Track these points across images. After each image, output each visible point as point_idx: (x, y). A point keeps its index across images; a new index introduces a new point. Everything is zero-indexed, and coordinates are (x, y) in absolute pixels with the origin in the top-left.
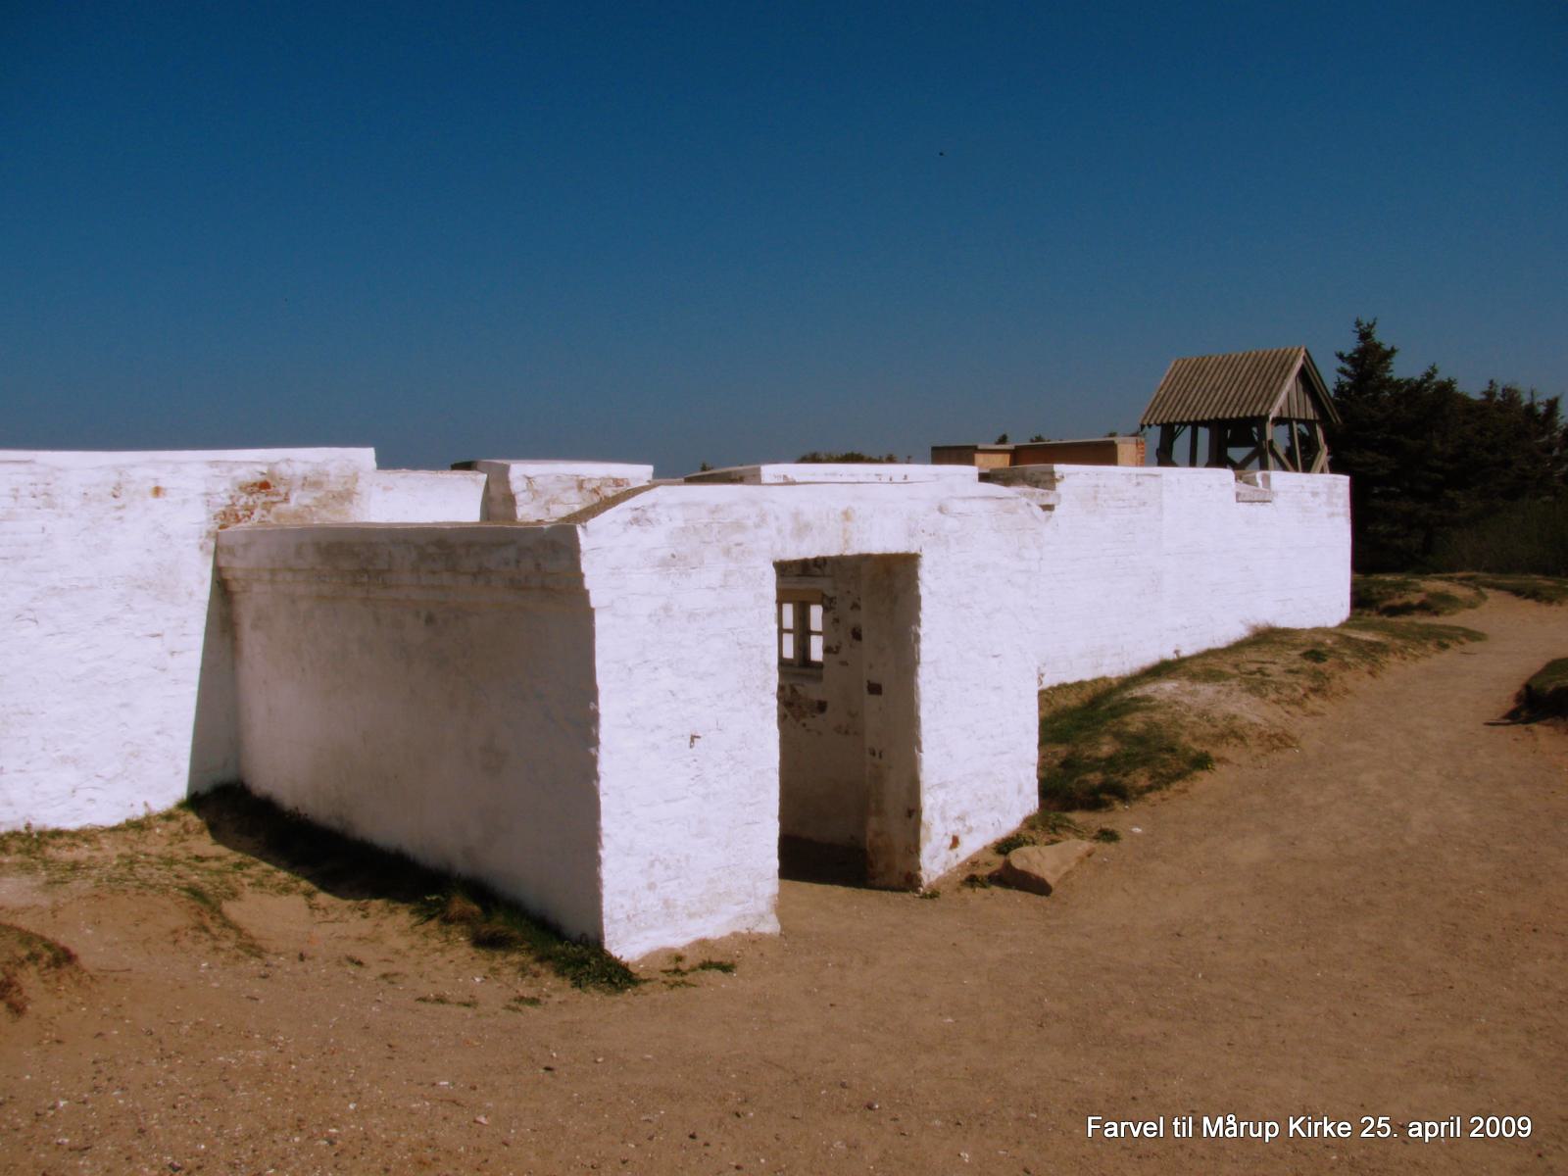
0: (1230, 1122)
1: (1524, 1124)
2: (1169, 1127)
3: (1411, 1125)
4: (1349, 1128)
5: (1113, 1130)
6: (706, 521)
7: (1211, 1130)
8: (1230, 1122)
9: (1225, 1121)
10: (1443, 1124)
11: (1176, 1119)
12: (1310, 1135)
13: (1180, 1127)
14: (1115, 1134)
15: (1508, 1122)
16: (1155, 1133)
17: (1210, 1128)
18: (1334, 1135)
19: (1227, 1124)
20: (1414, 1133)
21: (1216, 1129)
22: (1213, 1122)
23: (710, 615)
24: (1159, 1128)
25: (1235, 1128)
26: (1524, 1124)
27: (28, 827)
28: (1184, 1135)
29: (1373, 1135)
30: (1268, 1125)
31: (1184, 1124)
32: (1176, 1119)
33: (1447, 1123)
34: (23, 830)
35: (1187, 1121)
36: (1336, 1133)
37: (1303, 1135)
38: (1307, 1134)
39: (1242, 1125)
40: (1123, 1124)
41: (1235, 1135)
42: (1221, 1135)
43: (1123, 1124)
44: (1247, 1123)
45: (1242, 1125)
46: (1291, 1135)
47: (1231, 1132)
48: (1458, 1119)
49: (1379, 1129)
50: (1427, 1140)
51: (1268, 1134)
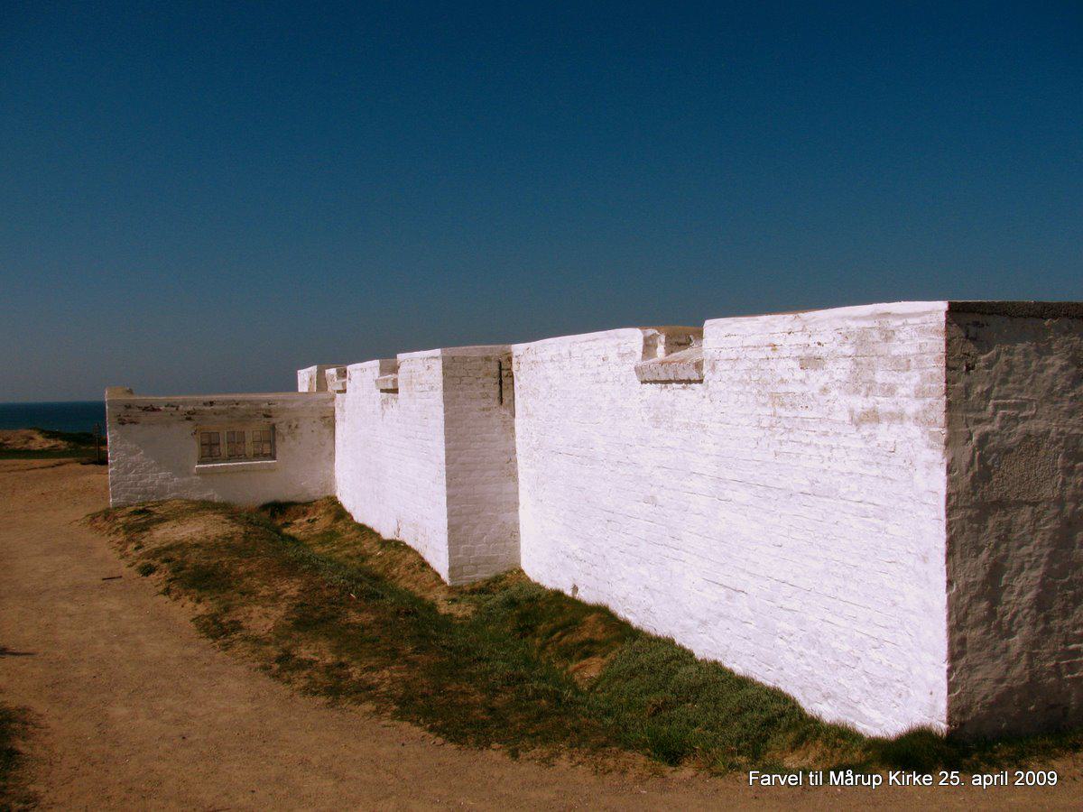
1: (1052, 776)
9: (845, 774)
13: (814, 778)
14: (769, 783)
16: (796, 783)
18: (920, 784)
22: (837, 776)
26: (1052, 776)
30: (874, 777)
35: (818, 774)
38: (901, 783)
39: (857, 776)
40: (774, 776)
43: (774, 776)
45: (857, 776)
51: (874, 783)
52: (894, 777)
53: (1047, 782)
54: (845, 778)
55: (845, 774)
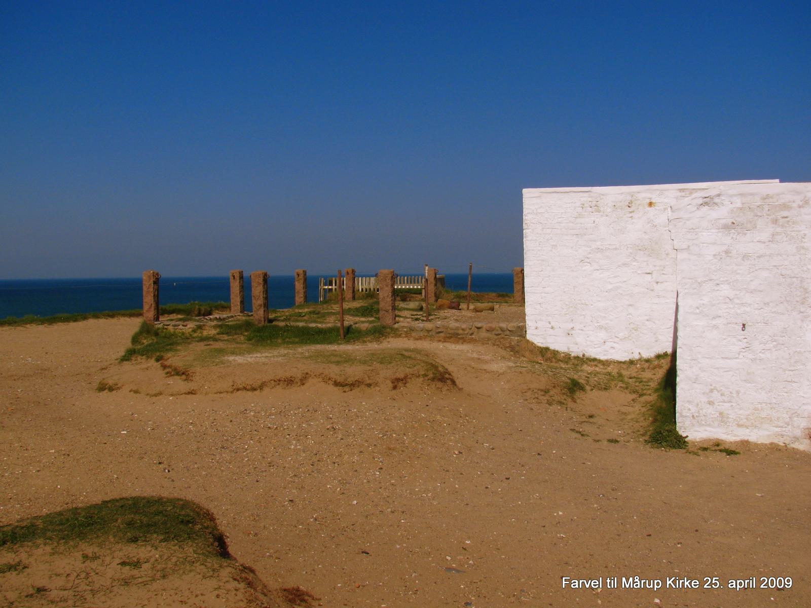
0: (636, 580)
1: (788, 581)
2: (605, 583)
3: (730, 582)
4: (698, 583)
5: (576, 584)
6: (758, 204)
7: (626, 584)
8: (636, 580)
9: (634, 580)
10: (746, 581)
11: (608, 579)
12: (677, 587)
13: (610, 583)
16: (597, 586)
17: (626, 583)
18: (690, 587)
19: (635, 581)
21: (629, 584)
22: (627, 580)
23: (759, 257)
24: (599, 583)
25: (639, 583)
26: (788, 581)
27: (584, 355)
28: (612, 587)
29: (710, 587)
30: (656, 582)
31: (612, 581)
32: (608, 579)
33: (749, 581)
34: (581, 356)
35: (614, 580)
36: (691, 586)
37: (674, 587)
38: (676, 586)
39: (643, 581)
40: (581, 581)
41: (639, 587)
42: (632, 587)
43: (581, 581)
44: (645, 581)
45: (643, 581)
46: (668, 587)
49: (713, 584)
51: (656, 586)
53: (784, 586)
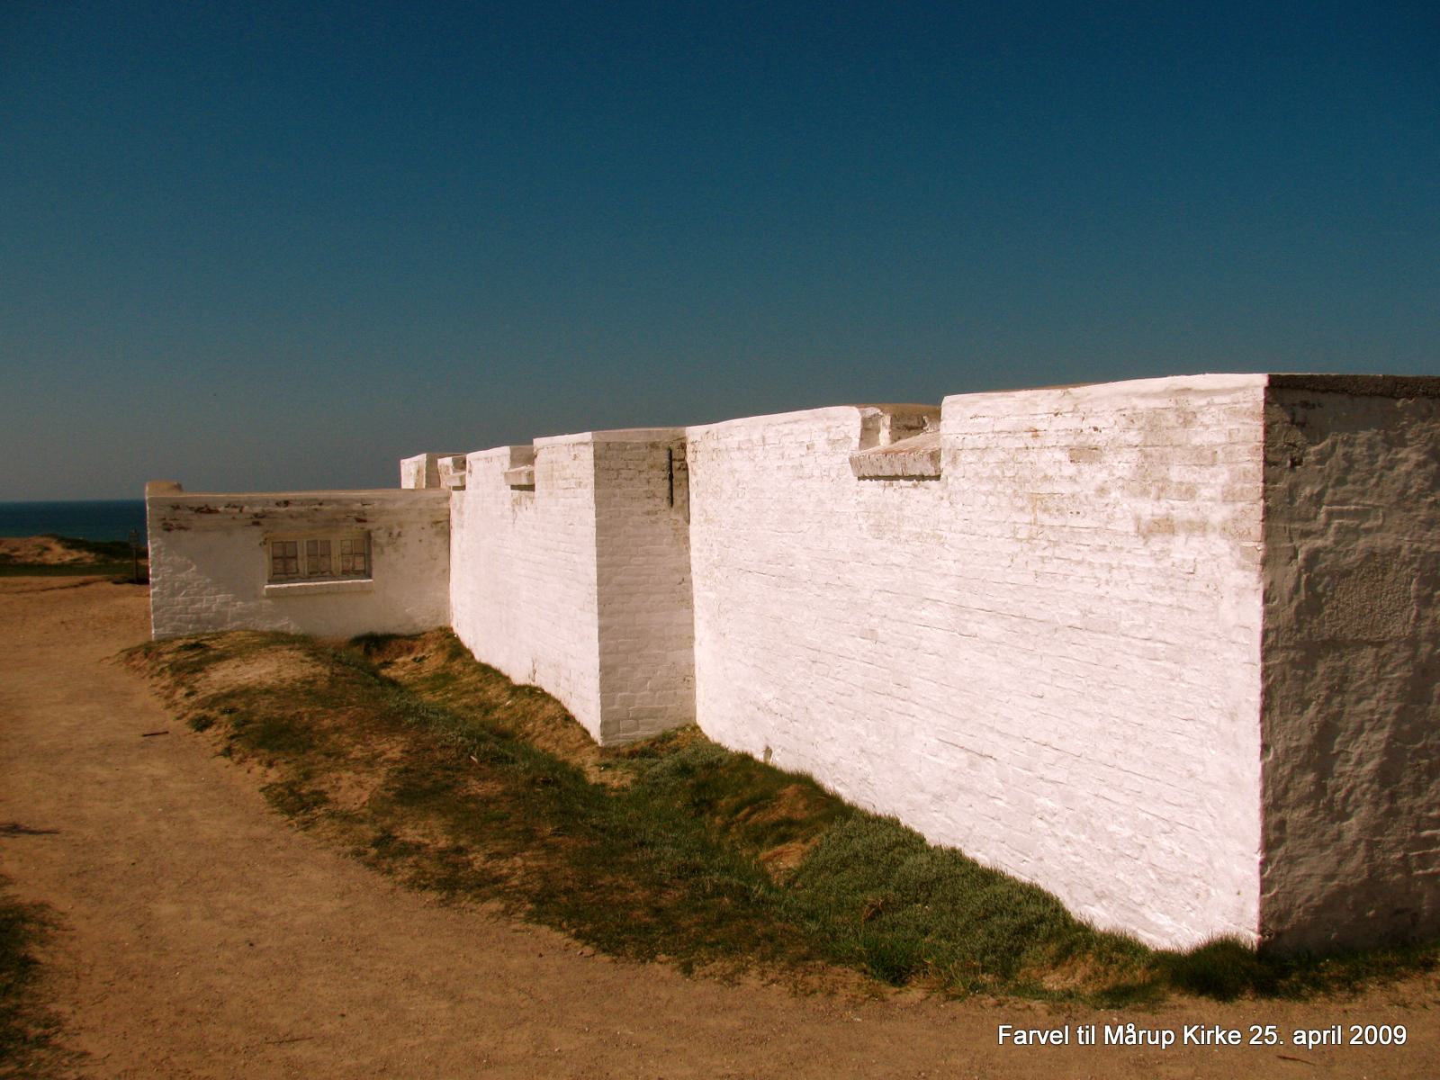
0: (1129, 1031)
1: (1400, 1032)
2: (1073, 1035)
4: (1239, 1036)
5: (1022, 1038)
8: (1129, 1031)
9: (1125, 1029)
10: (1325, 1033)
13: (1084, 1035)
14: (1024, 1042)
15: (1385, 1030)
18: (1225, 1043)
20: (1299, 1040)
22: (1114, 1031)
25: (1134, 1036)
26: (1400, 1032)
30: (1164, 1033)
35: (1090, 1030)
36: (1227, 1041)
37: (1197, 1043)
39: (1141, 1033)
40: (1031, 1033)
41: (1134, 1042)
42: (1121, 1042)
43: (1031, 1033)
45: (1141, 1033)
47: (1131, 1040)
48: (1339, 1027)
49: (1266, 1037)
50: (1310, 1047)
51: (1164, 1042)
52: (1190, 1033)
53: (1392, 1040)
54: (1125, 1035)
55: (1125, 1029)
